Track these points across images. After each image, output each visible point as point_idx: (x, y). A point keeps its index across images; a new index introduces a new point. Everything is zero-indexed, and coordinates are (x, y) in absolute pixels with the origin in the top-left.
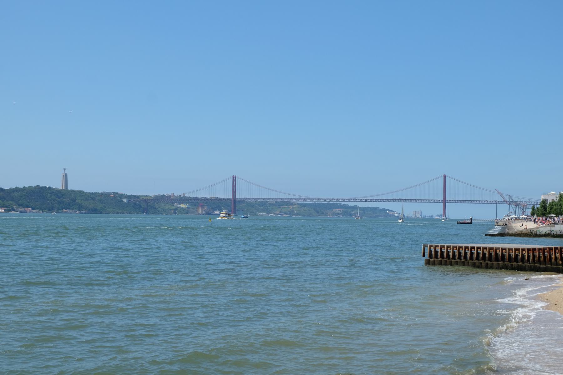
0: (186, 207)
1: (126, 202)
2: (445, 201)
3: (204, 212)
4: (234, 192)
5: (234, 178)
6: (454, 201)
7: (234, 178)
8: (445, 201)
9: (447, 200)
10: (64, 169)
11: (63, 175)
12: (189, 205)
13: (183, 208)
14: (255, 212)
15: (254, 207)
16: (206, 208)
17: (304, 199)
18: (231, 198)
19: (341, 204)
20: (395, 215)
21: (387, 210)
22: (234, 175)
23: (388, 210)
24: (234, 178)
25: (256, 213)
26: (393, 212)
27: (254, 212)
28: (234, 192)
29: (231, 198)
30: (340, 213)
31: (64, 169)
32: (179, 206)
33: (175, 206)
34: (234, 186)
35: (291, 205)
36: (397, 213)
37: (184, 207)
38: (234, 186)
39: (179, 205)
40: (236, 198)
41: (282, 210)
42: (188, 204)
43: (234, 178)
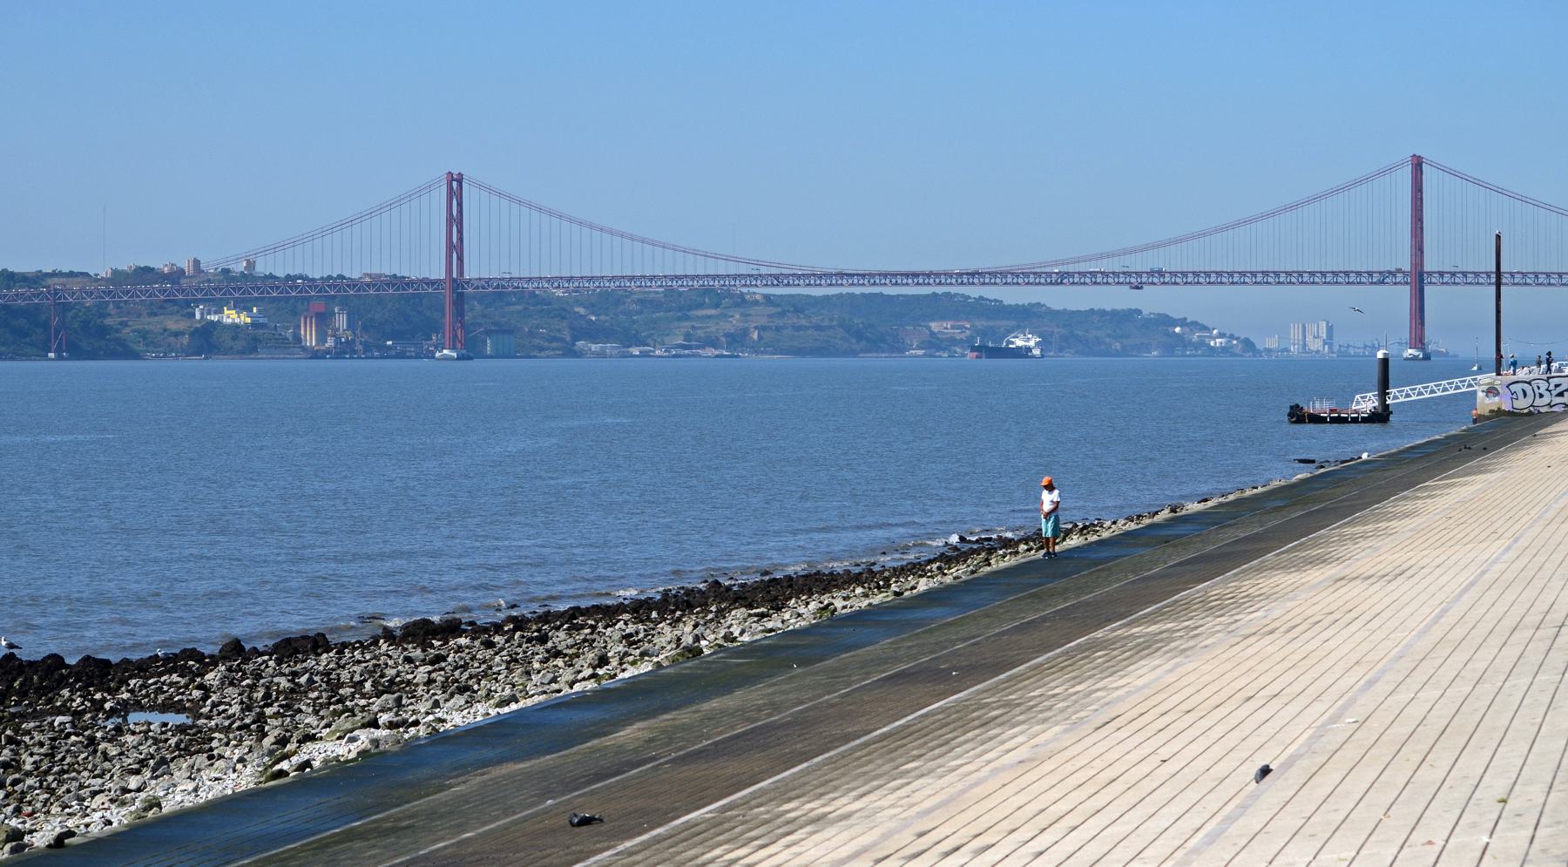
0: (248, 320)
2: (1418, 279)
3: (330, 343)
4: (455, 248)
6: (1376, 278)
8: (1418, 279)
9: (1430, 274)
12: (258, 311)
13: (235, 327)
14: (568, 339)
15: (564, 318)
16: (341, 321)
17: (776, 277)
18: (443, 277)
19: (969, 297)
20: (1212, 344)
21: (1175, 323)
22: (455, 172)
23: (1183, 322)
25: (574, 345)
26: (1204, 328)
27: (563, 340)
28: (455, 248)
29: (443, 277)
32: (214, 318)
33: (198, 316)
34: (455, 221)
35: (737, 305)
36: (1221, 335)
37: (237, 321)
38: (455, 221)
39: (216, 313)
41: (693, 327)
42: (255, 309)
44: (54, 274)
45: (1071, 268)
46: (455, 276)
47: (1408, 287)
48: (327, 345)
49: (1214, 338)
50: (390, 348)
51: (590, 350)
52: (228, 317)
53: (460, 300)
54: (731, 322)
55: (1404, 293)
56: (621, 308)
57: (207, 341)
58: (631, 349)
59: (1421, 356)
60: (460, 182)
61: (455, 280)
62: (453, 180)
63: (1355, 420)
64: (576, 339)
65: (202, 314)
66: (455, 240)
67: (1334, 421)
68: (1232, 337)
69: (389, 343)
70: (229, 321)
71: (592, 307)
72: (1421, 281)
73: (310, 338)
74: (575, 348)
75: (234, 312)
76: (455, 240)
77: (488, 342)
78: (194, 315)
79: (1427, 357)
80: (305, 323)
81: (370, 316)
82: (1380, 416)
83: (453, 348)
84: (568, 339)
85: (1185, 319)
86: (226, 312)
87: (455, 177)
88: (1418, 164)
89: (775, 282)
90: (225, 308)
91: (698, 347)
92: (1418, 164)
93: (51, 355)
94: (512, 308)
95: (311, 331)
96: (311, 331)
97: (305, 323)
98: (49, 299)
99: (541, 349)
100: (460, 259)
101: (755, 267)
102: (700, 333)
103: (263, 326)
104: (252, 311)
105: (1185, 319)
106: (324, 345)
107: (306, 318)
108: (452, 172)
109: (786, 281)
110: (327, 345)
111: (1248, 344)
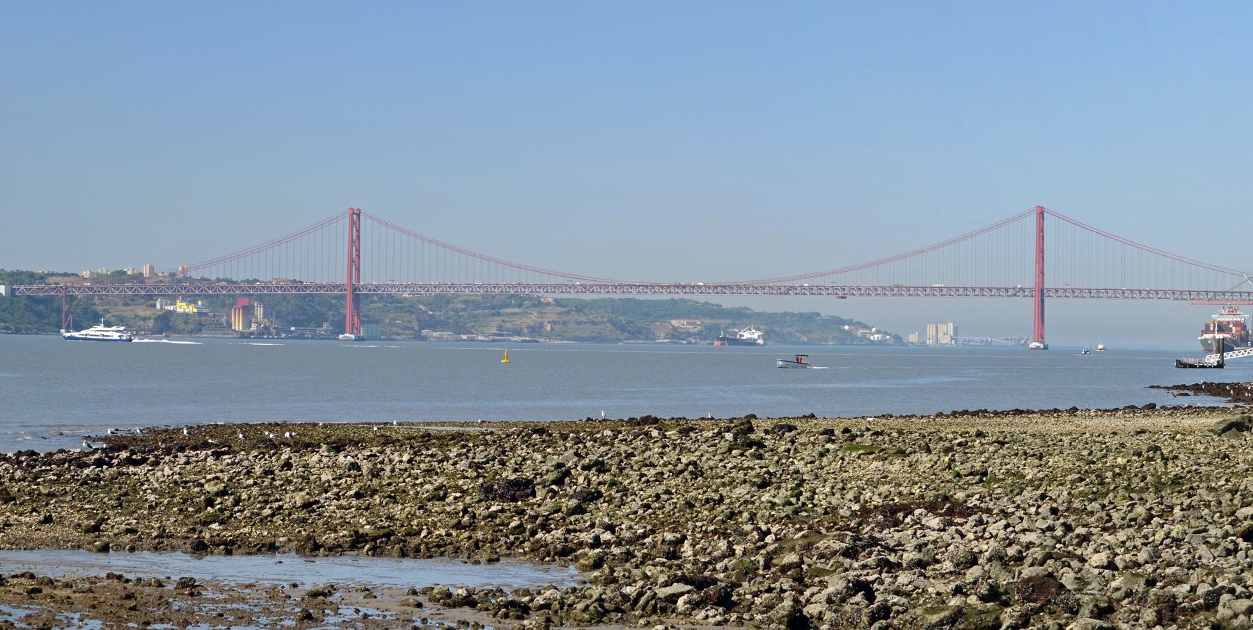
0: (195, 310)
2: (1041, 294)
4: (354, 263)
8: (1041, 294)
9: (1048, 290)
12: (203, 304)
14: (416, 328)
15: (413, 313)
16: (259, 312)
19: (698, 303)
20: (872, 338)
21: (844, 322)
22: (355, 208)
23: (850, 323)
25: (420, 332)
26: (865, 327)
27: (413, 329)
28: (354, 263)
30: (692, 331)
33: (158, 306)
34: (355, 242)
35: (534, 306)
36: (878, 332)
37: (187, 310)
38: (355, 242)
39: (171, 304)
41: (504, 321)
42: (200, 303)
43: (355, 216)
44: (52, 275)
45: (796, 284)
47: (1033, 300)
49: (873, 334)
50: (293, 332)
53: (357, 298)
55: (1030, 304)
56: (450, 306)
59: (1042, 346)
60: (358, 215)
62: (354, 213)
63: (1210, 367)
65: (161, 305)
67: (1200, 367)
68: (886, 333)
69: (293, 329)
70: (181, 310)
72: (1043, 295)
73: (238, 325)
78: (155, 306)
79: (1046, 348)
80: (235, 316)
82: (1220, 365)
84: (416, 328)
85: (852, 320)
86: (179, 303)
88: (1041, 213)
89: (584, 290)
91: (508, 335)
92: (1041, 213)
97: (235, 316)
100: (358, 270)
103: (205, 314)
105: (852, 320)
107: (235, 309)
109: (591, 290)
111: (898, 339)
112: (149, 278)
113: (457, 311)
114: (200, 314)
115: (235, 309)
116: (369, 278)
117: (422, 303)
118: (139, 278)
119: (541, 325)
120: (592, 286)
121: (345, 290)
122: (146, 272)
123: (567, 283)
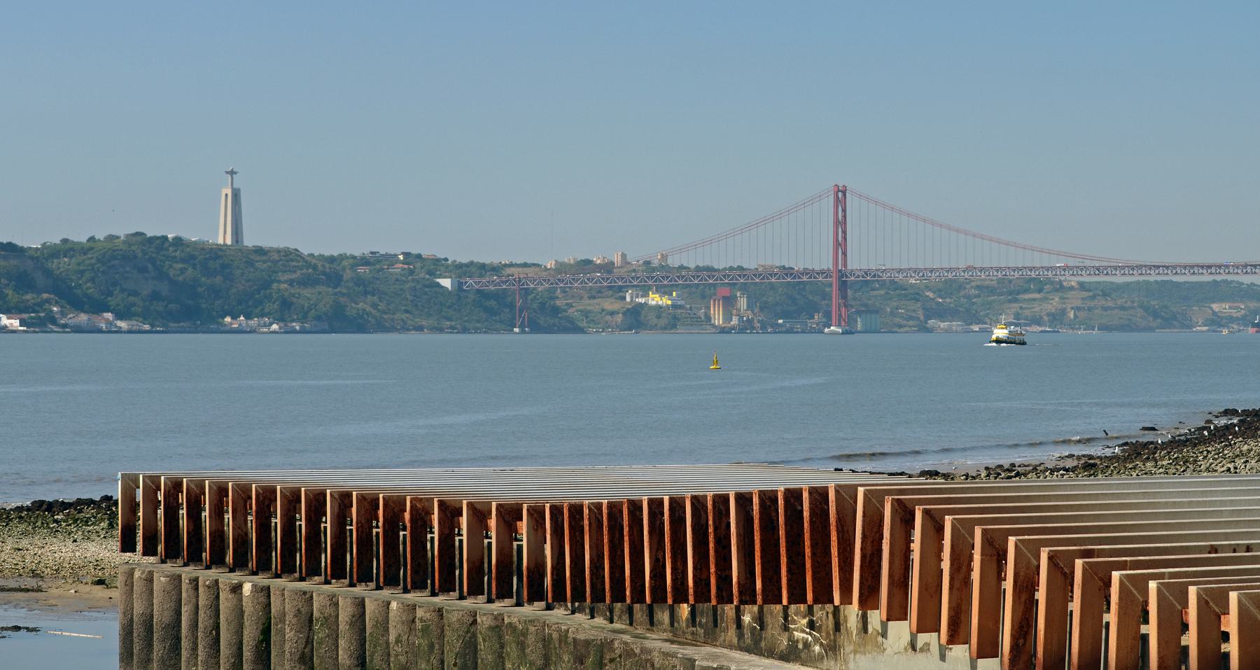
0: (669, 302)
1: (450, 289)
3: (735, 321)
4: (840, 245)
5: (840, 194)
7: (841, 195)
10: (227, 173)
11: (227, 195)
13: (659, 307)
14: (922, 318)
15: (918, 300)
16: (743, 303)
22: (841, 185)
24: (841, 195)
25: (926, 323)
27: (918, 318)
28: (840, 245)
31: (227, 173)
33: (628, 299)
34: (841, 223)
35: (1057, 290)
37: (660, 303)
38: (841, 223)
39: (642, 296)
40: (849, 267)
41: (1021, 308)
42: (674, 294)
44: (511, 265)
46: (840, 268)
48: (732, 323)
50: (781, 325)
51: (939, 327)
52: (653, 300)
53: (843, 286)
54: (1052, 304)
56: (962, 293)
57: (636, 318)
58: (972, 327)
61: (840, 271)
62: (839, 191)
64: (928, 318)
65: (632, 297)
66: (840, 239)
69: (781, 321)
70: (654, 303)
71: (939, 292)
73: (718, 319)
74: (928, 325)
75: (657, 296)
76: (840, 239)
77: (859, 320)
80: (714, 305)
81: (765, 299)
83: (839, 325)
86: (651, 295)
87: (840, 188)
89: (1097, 272)
90: (650, 293)
91: (1026, 325)
93: (516, 330)
94: (875, 293)
95: (719, 311)
96: (719, 311)
97: (714, 305)
98: (514, 285)
99: (900, 326)
100: (845, 254)
101: (1081, 260)
102: (1027, 312)
103: (680, 307)
104: (672, 295)
106: (729, 323)
107: (715, 301)
108: (838, 184)
109: (1105, 272)
110: (732, 323)
112: (621, 267)
113: (969, 297)
114: (674, 306)
115: (715, 301)
116: (858, 261)
117: (930, 290)
118: (608, 267)
119: (1063, 312)
120: (1106, 268)
121: (831, 277)
122: (617, 260)
123: (1078, 264)
